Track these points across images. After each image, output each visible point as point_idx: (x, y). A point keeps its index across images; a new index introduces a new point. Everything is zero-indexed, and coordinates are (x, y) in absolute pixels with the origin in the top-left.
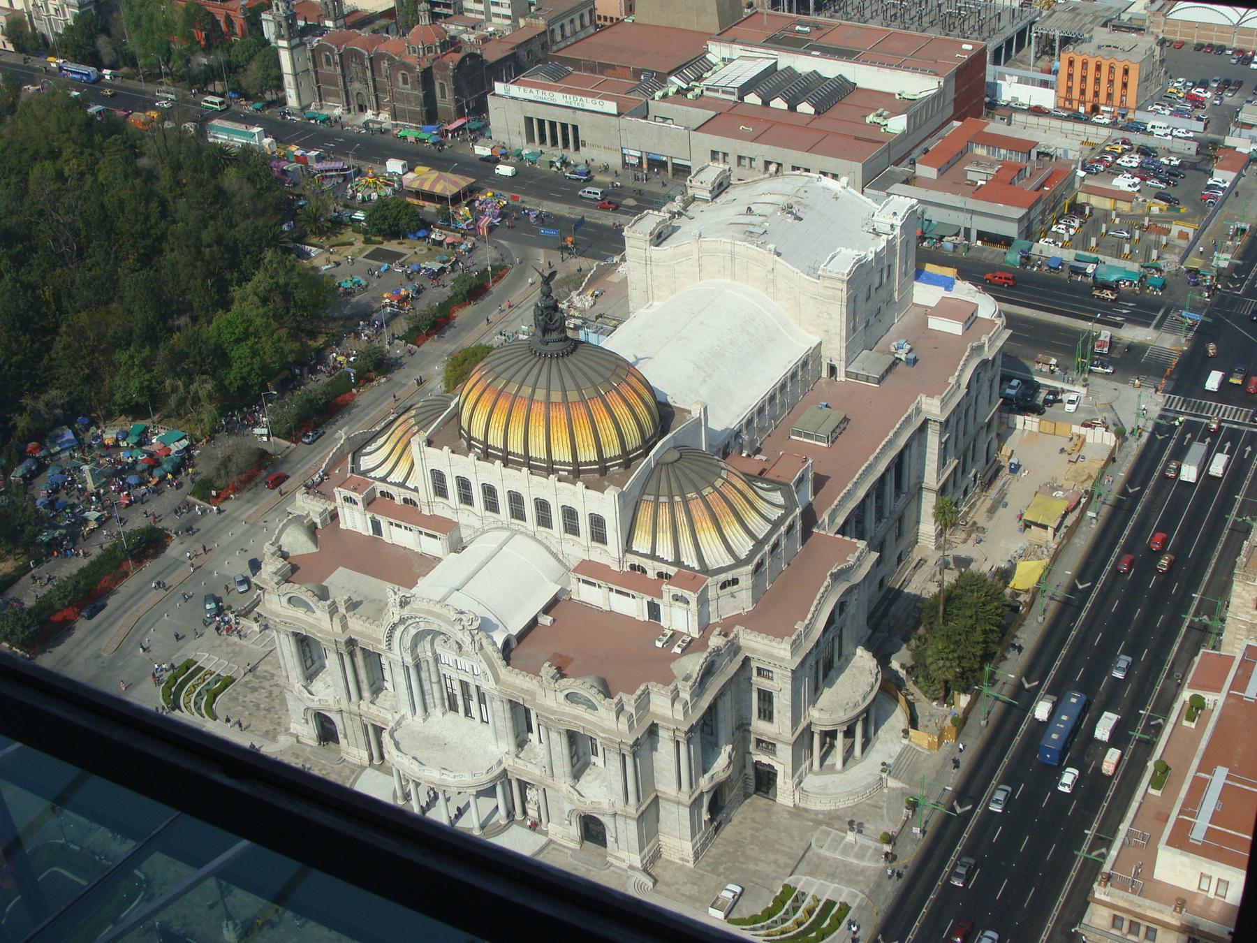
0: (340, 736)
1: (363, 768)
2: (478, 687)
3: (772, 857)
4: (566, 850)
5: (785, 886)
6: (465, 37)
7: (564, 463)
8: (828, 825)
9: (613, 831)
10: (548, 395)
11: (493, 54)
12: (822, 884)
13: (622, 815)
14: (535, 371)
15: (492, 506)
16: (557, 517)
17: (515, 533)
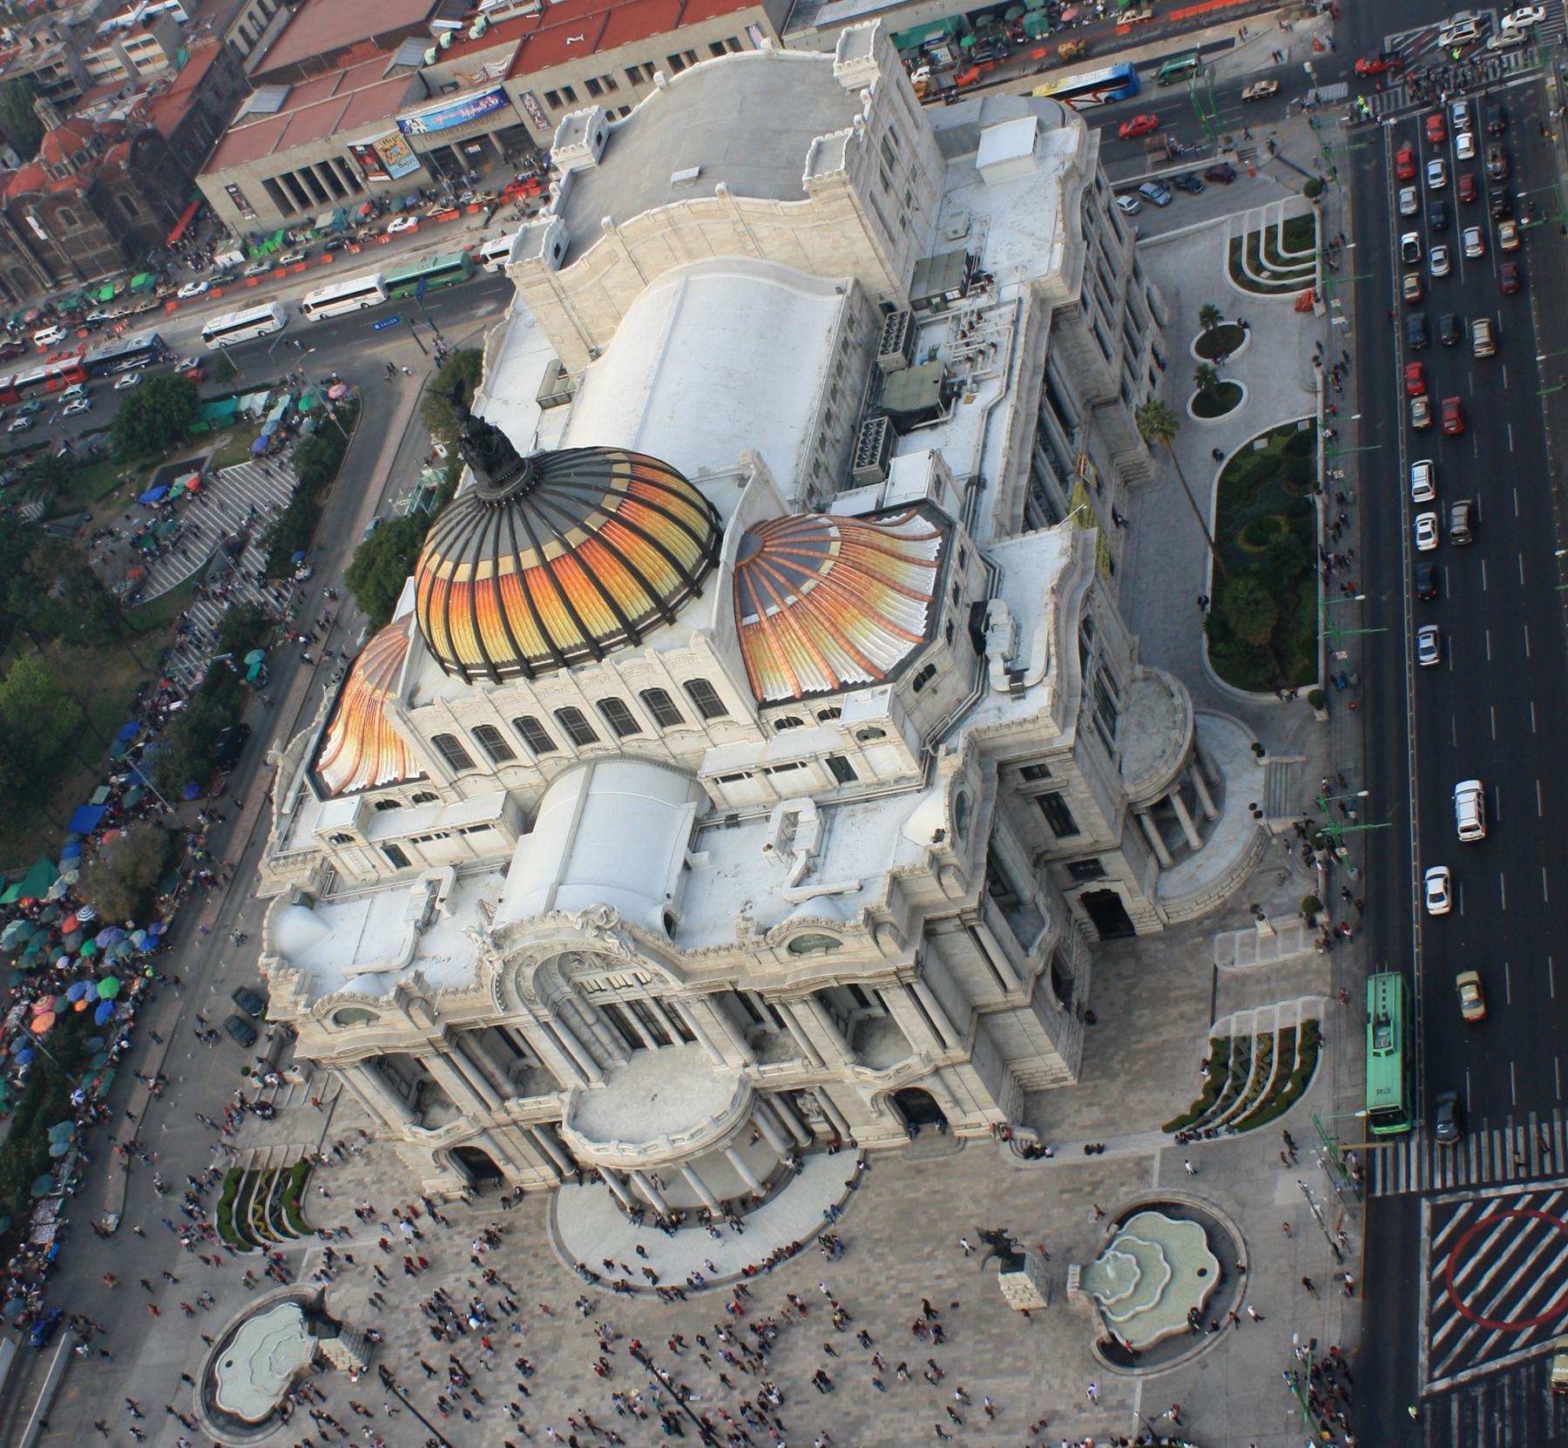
0: (500, 1164)
1: (554, 1190)
2: (657, 1000)
3: (1174, 1012)
4: (894, 1153)
5: (1214, 1042)
6: (118, 115)
7: (612, 634)
8: (1224, 929)
9: (945, 1093)
10: (540, 553)
11: (170, 117)
12: (1262, 1013)
13: (947, 1066)
14: (505, 531)
15: (541, 744)
16: (639, 712)
17: (593, 763)
